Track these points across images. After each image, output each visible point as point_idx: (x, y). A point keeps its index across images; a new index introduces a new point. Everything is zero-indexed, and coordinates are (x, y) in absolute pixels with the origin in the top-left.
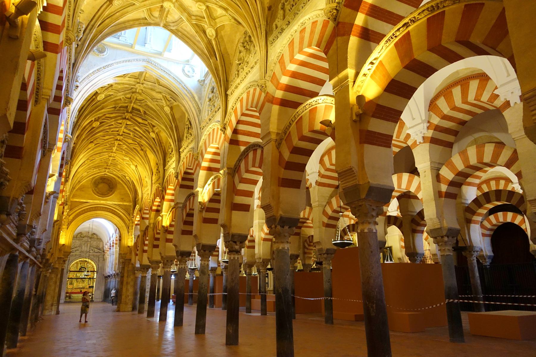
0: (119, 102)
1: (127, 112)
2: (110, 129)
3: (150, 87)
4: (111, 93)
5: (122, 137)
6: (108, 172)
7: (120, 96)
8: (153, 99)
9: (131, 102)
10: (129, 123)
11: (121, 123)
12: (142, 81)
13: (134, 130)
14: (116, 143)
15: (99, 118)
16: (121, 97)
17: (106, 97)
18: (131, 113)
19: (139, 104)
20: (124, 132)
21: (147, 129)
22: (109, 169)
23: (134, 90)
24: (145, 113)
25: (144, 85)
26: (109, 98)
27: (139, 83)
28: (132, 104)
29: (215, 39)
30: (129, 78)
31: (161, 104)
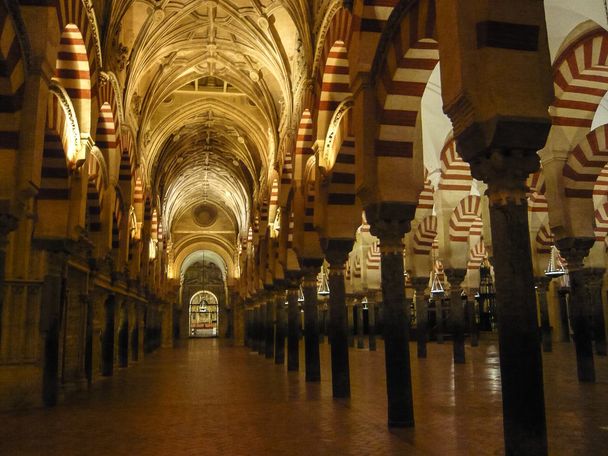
0: (195, 137)
1: (207, 145)
2: (195, 161)
3: (219, 122)
4: (185, 133)
5: (209, 167)
6: (207, 199)
7: (195, 132)
8: (226, 130)
9: (207, 137)
10: (211, 153)
11: (204, 154)
12: (210, 117)
13: (218, 159)
14: (206, 172)
15: (182, 154)
16: (196, 134)
17: (182, 136)
18: (210, 144)
19: (216, 136)
20: (210, 161)
21: (229, 157)
22: (207, 196)
23: (206, 126)
24: (223, 144)
25: (214, 121)
26: (184, 137)
27: (208, 120)
28: (209, 138)
29: (259, 80)
30: (198, 118)
31: (235, 134)
